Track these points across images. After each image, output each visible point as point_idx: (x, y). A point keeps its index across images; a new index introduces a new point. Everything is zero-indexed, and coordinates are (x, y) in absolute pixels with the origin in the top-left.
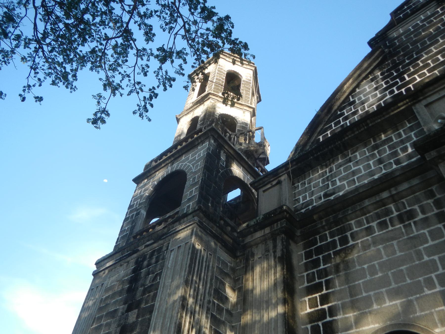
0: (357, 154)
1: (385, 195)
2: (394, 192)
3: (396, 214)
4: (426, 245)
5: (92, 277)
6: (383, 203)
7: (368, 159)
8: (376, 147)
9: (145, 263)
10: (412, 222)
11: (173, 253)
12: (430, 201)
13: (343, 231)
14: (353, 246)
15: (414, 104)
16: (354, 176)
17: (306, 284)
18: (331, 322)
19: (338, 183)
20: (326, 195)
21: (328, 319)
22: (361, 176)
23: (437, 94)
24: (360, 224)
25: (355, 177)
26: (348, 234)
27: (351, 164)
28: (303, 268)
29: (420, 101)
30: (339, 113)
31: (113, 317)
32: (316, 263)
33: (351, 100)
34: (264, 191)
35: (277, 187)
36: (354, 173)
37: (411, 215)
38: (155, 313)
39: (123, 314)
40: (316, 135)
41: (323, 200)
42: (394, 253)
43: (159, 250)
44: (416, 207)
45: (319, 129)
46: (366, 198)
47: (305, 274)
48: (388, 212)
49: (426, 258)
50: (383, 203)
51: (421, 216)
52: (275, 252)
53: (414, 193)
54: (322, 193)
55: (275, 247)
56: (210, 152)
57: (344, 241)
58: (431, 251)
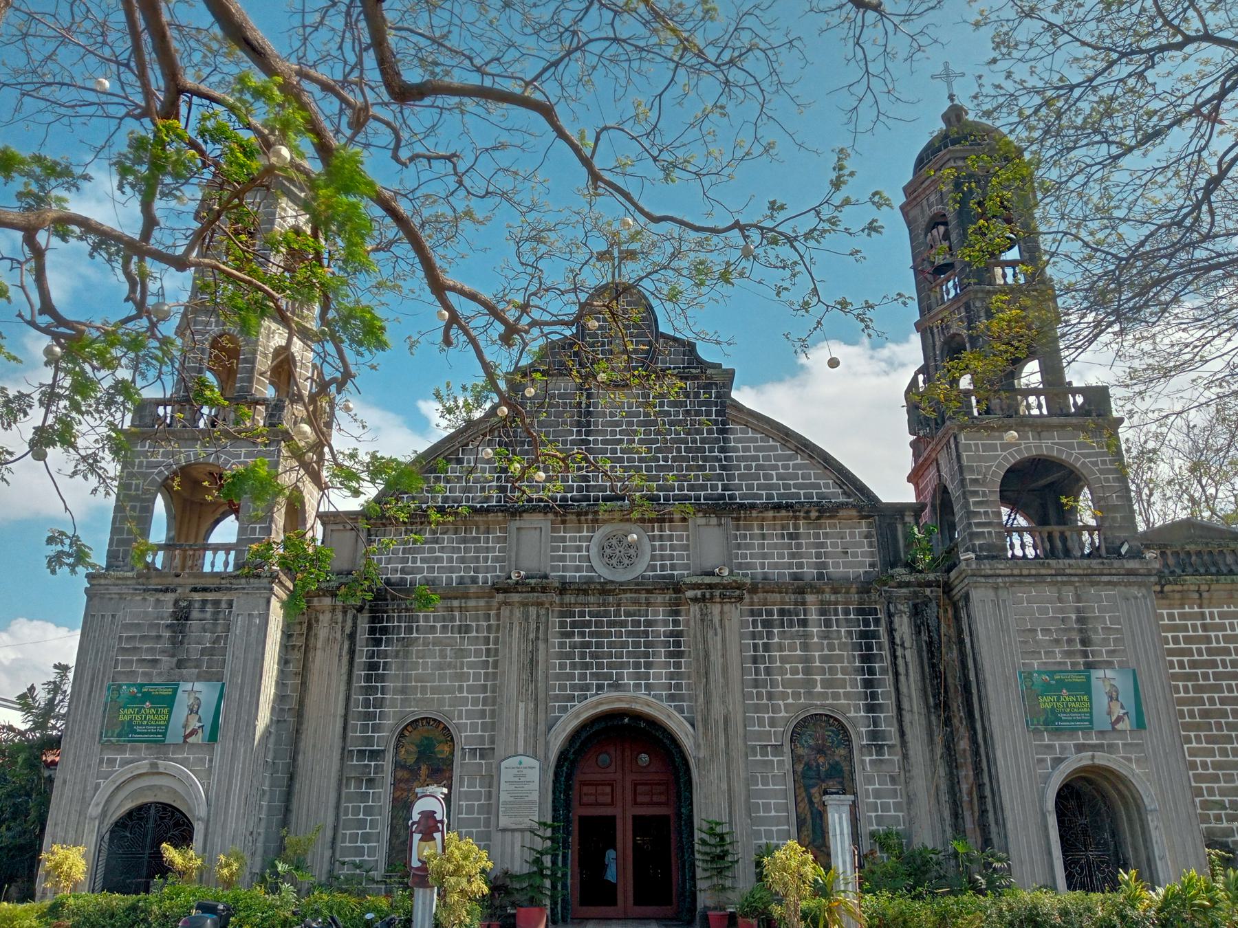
1: (456, 603)
6: (452, 609)
7: (454, 550)
8: (464, 541)
12: (485, 624)
13: (411, 619)
17: (364, 659)
19: (419, 564)
20: (403, 571)
24: (426, 619)
26: (414, 625)
28: (364, 643)
31: (154, 667)
32: (378, 642)
37: (468, 629)
44: (474, 624)
48: (453, 619)
50: (452, 609)
51: (474, 634)
55: (344, 621)
57: (409, 630)
58: (472, 665)
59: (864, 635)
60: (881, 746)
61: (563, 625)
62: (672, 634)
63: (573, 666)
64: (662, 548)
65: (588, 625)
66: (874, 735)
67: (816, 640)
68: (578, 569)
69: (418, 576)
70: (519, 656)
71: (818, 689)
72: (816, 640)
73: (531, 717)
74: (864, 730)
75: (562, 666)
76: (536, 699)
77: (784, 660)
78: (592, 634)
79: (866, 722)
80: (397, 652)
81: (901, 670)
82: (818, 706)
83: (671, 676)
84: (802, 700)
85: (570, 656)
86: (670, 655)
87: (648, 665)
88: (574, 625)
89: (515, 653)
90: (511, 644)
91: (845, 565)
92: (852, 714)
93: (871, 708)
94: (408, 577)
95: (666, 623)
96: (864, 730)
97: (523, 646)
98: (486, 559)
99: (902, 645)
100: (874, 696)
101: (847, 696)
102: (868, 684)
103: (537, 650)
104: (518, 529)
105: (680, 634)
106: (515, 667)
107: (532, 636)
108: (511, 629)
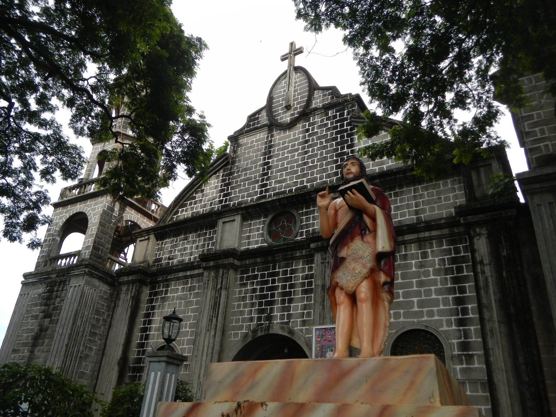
0: (191, 235)
1: (188, 273)
2: (192, 274)
3: (190, 285)
4: (192, 307)
5: (21, 285)
7: (194, 242)
8: (199, 236)
9: (56, 288)
10: (193, 292)
11: (72, 288)
13: (168, 286)
14: (169, 297)
15: (219, 218)
16: (184, 251)
17: (145, 312)
18: (148, 334)
19: (176, 253)
20: (169, 259)
21: (148, 333)
22: (187, 253)
23: (229, 218)
25: (184, 252)
27: (185, 241)
28: (146, 302)
29: (222, 218)
30: (194, 195)
33: (203, 188)
34: (140, 241)
35: (146, 241)
36: (185, 249)
38: (59, 324)
39: (41, 319)
40: (178, 207)
41: (167, 261)
42: (181, 307)
43: (65, 281)
44: (197, 285)
45: (180, 204)
46: (180, 272)
47: (146, 305)
48: (187, 283)
49: (190, 314)
51: (197, 291)
52: (131, 292)
53: (199, 276)
54: (168, 256)
55: (132, 289)
56: (106, 209)
59: (453, 261)
60: (471, 356)
61: (242, 279)
62: (307, 277)
63: (245, 306)
64: (308, 219)
65: (256, 277)
66: (465, 346)
67: (414, 269)
68: (257, 242)
69: (175, 260)
70: (210, 301)
72: (414, 269)
73: (212, 340)
74: (455, 341)
75: (239, 306)
76: (216, 329)
78: (258, 284)
79: (457, 334)
80: (160, 305)
81: (481, 284)
82: (413, 323)
83: (305, 307)
84: (402, 319)
85: (244, 299)
86: (305, 292)
87: (291, 301)
88: (248, 278)
89: (208, 299)
90: (207, 293)
91: (439, 208)
92: (445, 328)
93: (461, 322)
94: (171, 261)
95: (303, 270)
96: (455, 341)
97: (213, 294)
98: (208, 244)
99: (482, 262)
101: (441, 313)
102: (459, 301)
103: (220, 296)
104: (224, 223)
105: (312, 276)
106: (207, 308)
107: (219, 286)
108: (208, 283)
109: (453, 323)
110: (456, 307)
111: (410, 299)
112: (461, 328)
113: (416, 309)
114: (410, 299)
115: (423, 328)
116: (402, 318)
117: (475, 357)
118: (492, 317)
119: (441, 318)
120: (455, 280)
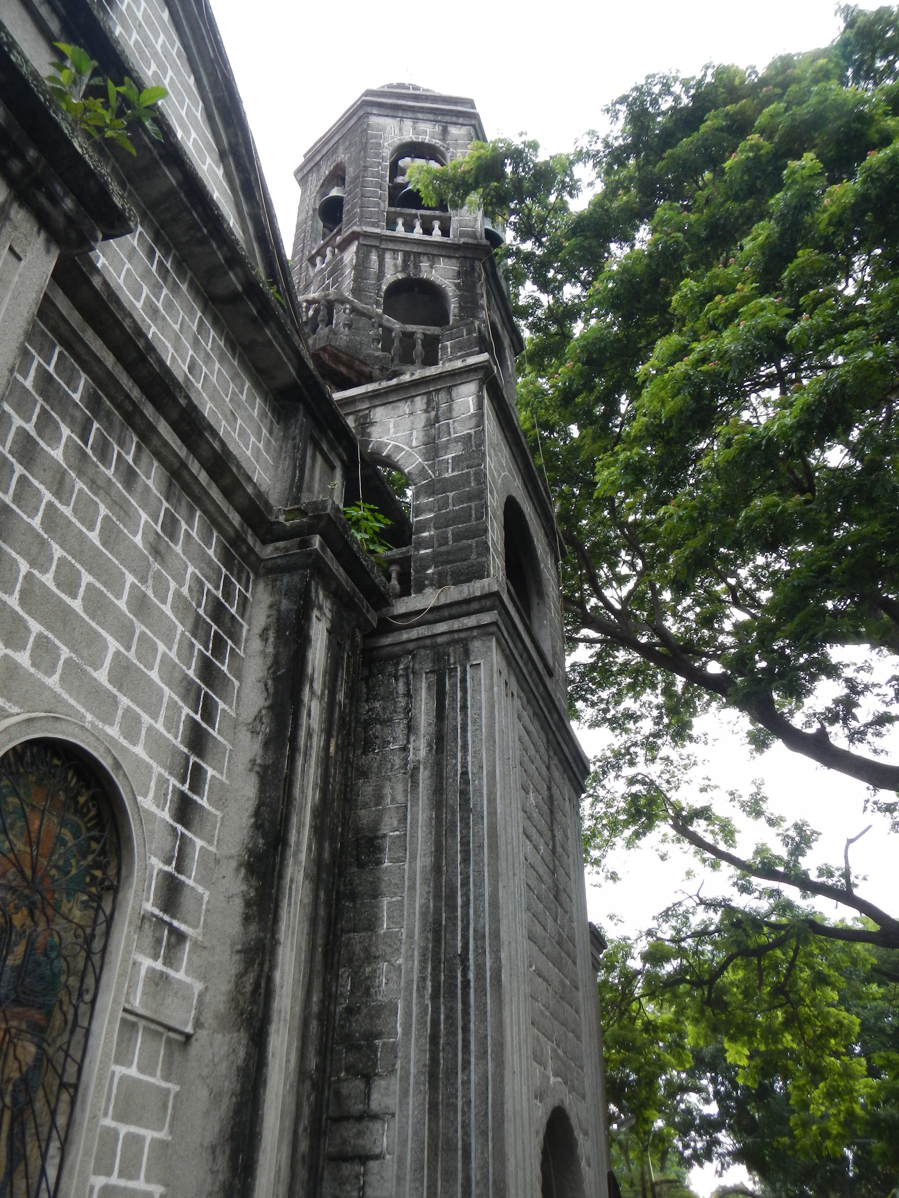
60: (179, 937)
71: (102, 676)
77: (52, 517)
81: (302, 742)
100: (197, 777)
101: (155, 741)
109: (169, 797)
110: (186, 750)
111: (100, 630)
112: (179, 827)
113: (102, 676)
114: (100, 630)
115: (107, 763)
116: (56, 677)
117: (188, 945)
118: (298, 843)
119: (151, 762)
120: (208, 671)
